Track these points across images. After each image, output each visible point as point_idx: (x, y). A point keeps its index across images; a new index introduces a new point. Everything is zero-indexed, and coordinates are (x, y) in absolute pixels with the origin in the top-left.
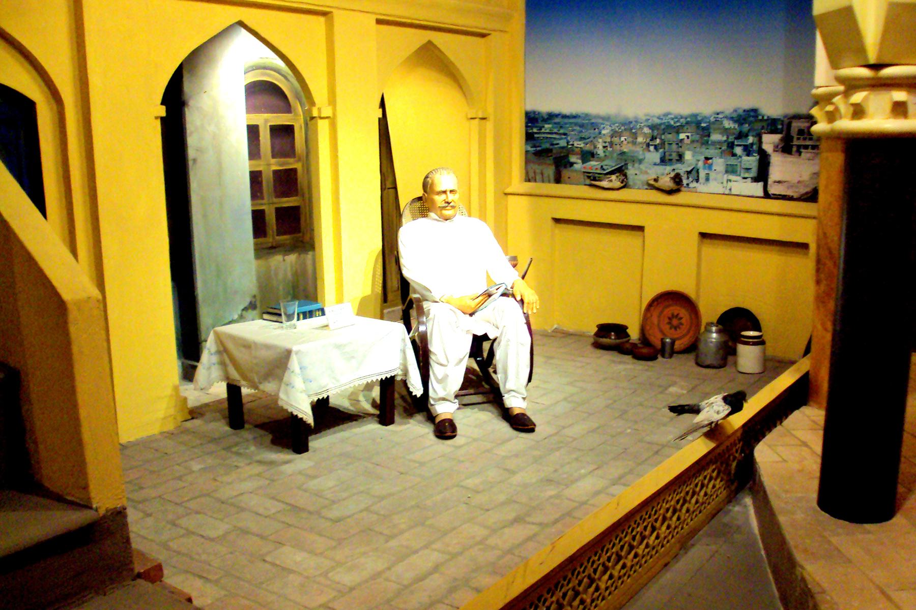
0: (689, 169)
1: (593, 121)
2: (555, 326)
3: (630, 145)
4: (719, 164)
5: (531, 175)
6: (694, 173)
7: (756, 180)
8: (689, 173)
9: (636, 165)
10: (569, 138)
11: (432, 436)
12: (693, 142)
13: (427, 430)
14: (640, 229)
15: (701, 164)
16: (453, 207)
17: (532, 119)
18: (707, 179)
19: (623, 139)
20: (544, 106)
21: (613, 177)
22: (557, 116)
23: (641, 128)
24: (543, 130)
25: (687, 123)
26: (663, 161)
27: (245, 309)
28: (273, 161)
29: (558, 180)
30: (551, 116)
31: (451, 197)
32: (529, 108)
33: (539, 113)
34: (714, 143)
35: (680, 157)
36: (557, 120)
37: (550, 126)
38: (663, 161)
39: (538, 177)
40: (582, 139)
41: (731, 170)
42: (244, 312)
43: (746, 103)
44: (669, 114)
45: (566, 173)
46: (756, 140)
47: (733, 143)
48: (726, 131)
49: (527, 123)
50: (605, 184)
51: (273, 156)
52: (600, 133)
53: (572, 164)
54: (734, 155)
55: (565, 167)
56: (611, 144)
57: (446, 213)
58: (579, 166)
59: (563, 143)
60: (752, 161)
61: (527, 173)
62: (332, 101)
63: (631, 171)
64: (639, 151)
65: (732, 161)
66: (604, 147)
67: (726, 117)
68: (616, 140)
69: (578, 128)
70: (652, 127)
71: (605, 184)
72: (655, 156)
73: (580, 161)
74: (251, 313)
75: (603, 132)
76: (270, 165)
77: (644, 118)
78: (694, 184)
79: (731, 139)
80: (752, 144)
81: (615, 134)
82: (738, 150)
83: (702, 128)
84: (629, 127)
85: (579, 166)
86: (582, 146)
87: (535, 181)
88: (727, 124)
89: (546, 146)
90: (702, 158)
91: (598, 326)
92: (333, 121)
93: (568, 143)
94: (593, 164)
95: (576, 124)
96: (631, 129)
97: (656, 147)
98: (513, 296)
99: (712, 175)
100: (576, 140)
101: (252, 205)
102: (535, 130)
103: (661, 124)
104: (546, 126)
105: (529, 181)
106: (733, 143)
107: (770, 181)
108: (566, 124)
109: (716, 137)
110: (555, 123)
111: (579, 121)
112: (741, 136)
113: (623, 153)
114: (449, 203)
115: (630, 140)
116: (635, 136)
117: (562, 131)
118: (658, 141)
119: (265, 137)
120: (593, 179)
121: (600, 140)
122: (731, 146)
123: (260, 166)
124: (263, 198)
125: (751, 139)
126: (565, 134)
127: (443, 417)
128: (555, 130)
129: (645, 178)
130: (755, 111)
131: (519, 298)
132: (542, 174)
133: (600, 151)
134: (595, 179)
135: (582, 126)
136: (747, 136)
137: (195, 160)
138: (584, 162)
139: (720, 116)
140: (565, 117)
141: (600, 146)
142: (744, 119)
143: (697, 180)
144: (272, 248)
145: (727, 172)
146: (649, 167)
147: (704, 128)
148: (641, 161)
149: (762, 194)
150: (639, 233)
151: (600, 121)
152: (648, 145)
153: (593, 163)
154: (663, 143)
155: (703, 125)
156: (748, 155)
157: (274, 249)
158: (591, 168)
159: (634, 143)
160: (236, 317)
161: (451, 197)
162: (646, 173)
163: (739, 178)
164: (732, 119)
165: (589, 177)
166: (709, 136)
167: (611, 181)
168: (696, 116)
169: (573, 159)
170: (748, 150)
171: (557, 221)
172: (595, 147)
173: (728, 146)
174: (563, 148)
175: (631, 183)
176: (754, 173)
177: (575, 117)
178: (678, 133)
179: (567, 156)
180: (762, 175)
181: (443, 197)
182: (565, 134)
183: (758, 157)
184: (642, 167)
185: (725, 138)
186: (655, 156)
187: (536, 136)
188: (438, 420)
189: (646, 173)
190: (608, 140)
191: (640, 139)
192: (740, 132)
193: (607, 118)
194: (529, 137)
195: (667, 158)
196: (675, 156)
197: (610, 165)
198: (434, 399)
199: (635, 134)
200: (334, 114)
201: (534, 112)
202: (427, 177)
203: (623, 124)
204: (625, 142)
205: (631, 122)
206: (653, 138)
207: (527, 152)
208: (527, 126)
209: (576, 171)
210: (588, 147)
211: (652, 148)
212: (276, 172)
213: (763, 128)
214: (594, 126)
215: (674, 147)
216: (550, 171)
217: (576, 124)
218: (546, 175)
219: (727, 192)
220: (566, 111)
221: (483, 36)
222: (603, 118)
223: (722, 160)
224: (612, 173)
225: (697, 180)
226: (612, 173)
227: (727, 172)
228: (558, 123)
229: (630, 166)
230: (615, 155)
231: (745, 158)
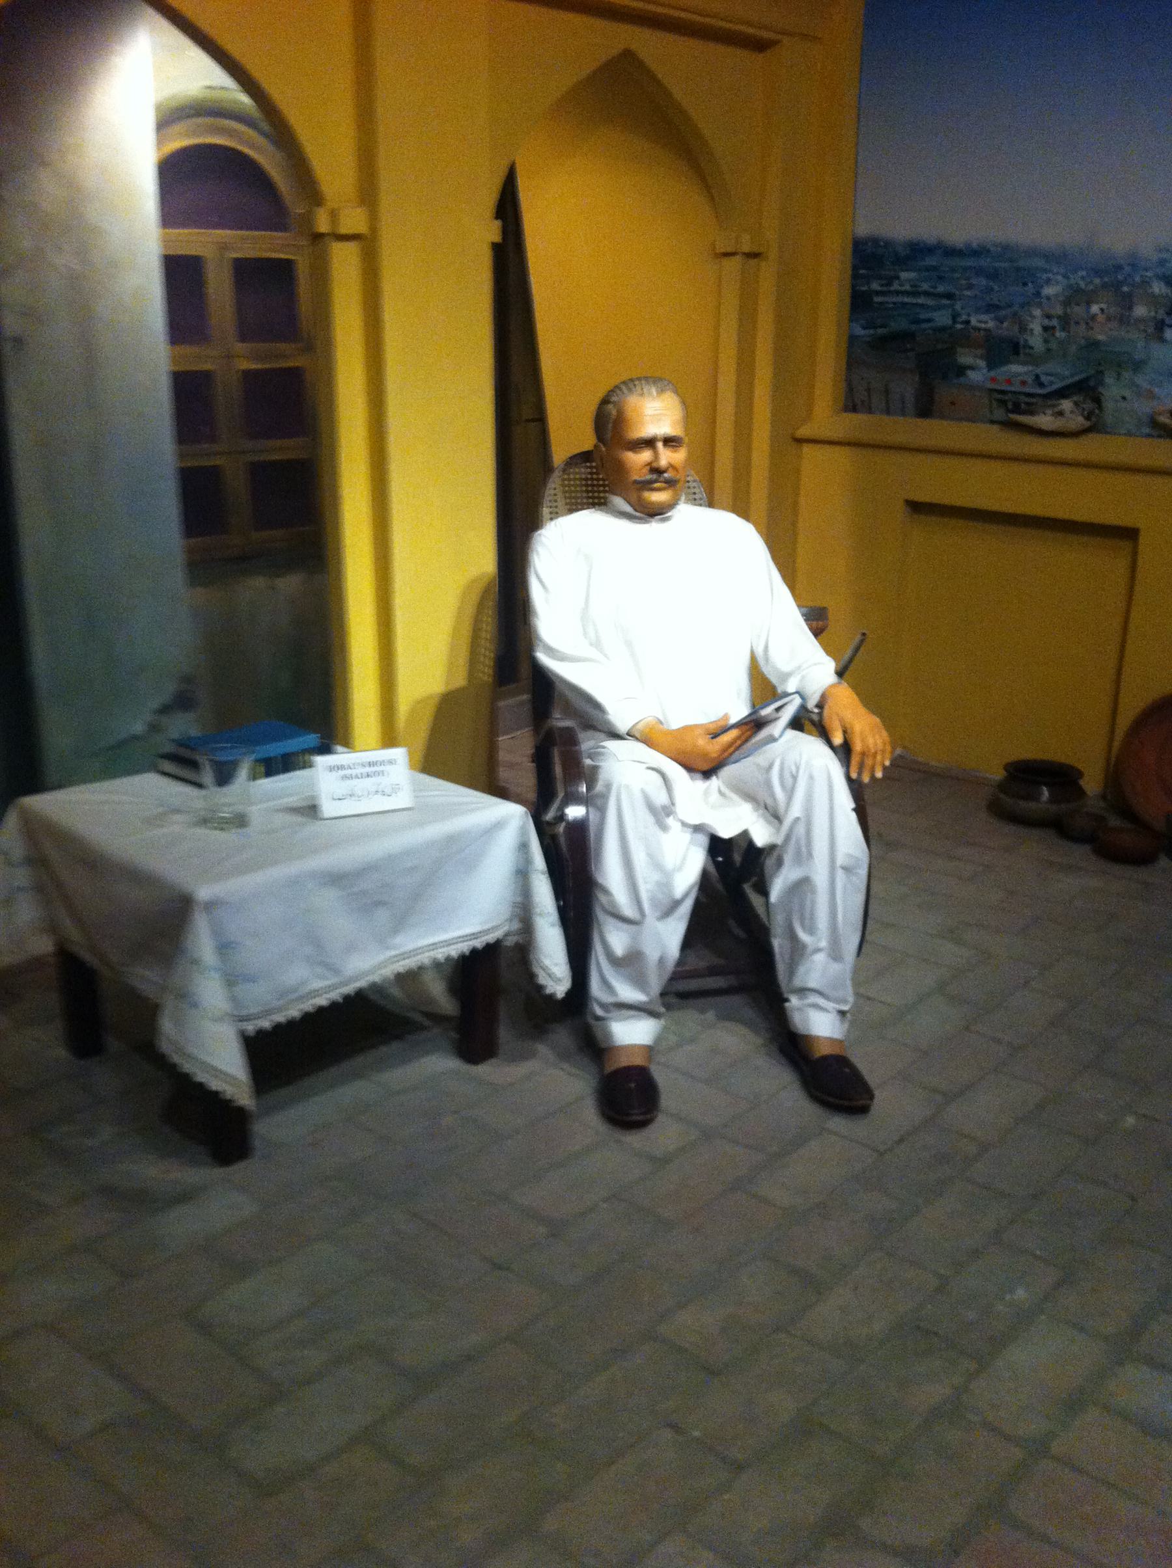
1: (1021, 263)
3: (1114, 324)
9: (1126, 375)
10: (958, 307)
11: (590, 1113)
14: (1130, 534)
16: (671, 483)
17: (870, 258)
19: (1095, 309)
20: (902, 223)
21: (1066, 405)
23: (1146, 283)
24: (896, 286)
27: (165, 710)
28: (240, 347)
29: (925, 409)
30: (917, 251)
31: (666, 457)
32: (863, 229)
33: (888, 244)
36: (930, 261)
37: (912, 275)
40: (991, 308)
49: (855, 268)
50: (1044, 420)
51: (243, 338)
52: (1038, 294)
53: (961, 370)
57: (658, 497)
58: (979, 374)
59: (942, 318)
61: (850, 390)
62: (368, 194)
63: (1112, 390)
66: (1046, 329)
68: (1078, 310)
69: (983, 282)
71: (1044, 420)
73: (982, 363)
76: (233, 358)
77: (1155, 257)
81: (1076, 296)
84: (1116, 280)
85: (979, 374)
86: (991, 325)
87: (870, 411)
89: (900, 324)
91: (1007, 767)
92: (368, 245)
93: (955, 317)
95: (979, 272)
96: (1117, 286)
98: (824, 733)
100: (978, 310)
101: (182, 456)
102: (875, 286)
104: (904, 275)
108: (953, 270)
110: (927, 269)
111: (984, 262)
113: (1094, 345)
114: (658, 471)
116: (1127, 302)
117: (941, 289)
119: (219, 288)
120: (1012, 409)
121: (1037, 312)
123: (202, 359)
124: (213, 439)
126: (949, 296)
127: (624, 1061)
128: (925, 286)
129: (1144, 407)
131: (838, 740)
132: (887, 392)
133: (1036, 340)
134: (1017, 409)
135: (994, 275)
138: (990, 367)
140: (951, 252)
148: (1138, 366)
150: (1126, 545)
151: (1039, 263)
153: (1015, 368)
157: (245, 562)
158: (1009, 382)
160: (138, 728)
161: (666, 457)
162: (1151, 396)
165: (1002, 403)
167: (1061, 414)
169: (965, 357)
171: (916, 507)
172: (1023, 329)
174: (943, 329)
175: (1109, 419)
181: (646, 456)
184: (1141, 380)
188: (610, 1067)
189: (1151, 396)
190: (1059, 311)
191: (1140, 311)
193: (1058, 258)
194: (860, 303)
197: (1060, 373)
198: (604, 1006)
199: (1129, 295)
200: (374, 229)
201: (875, 241)
202: (605, 401)
203: (1097, 272)
204: (1101, 318)
205: (1119, 268)
207: (852, 339)
208: (855, 276)
209: (972, 387)
210: (1008, 329)
212: (247, 374)
214: (1025, 276)
216: (906, 387)
217: (979, 272)
221: (760, 46)
222: (1048, 256)
224: (1062, 393)
228: (935, 268)
229: (1109, 380)
230: (1073, 348)
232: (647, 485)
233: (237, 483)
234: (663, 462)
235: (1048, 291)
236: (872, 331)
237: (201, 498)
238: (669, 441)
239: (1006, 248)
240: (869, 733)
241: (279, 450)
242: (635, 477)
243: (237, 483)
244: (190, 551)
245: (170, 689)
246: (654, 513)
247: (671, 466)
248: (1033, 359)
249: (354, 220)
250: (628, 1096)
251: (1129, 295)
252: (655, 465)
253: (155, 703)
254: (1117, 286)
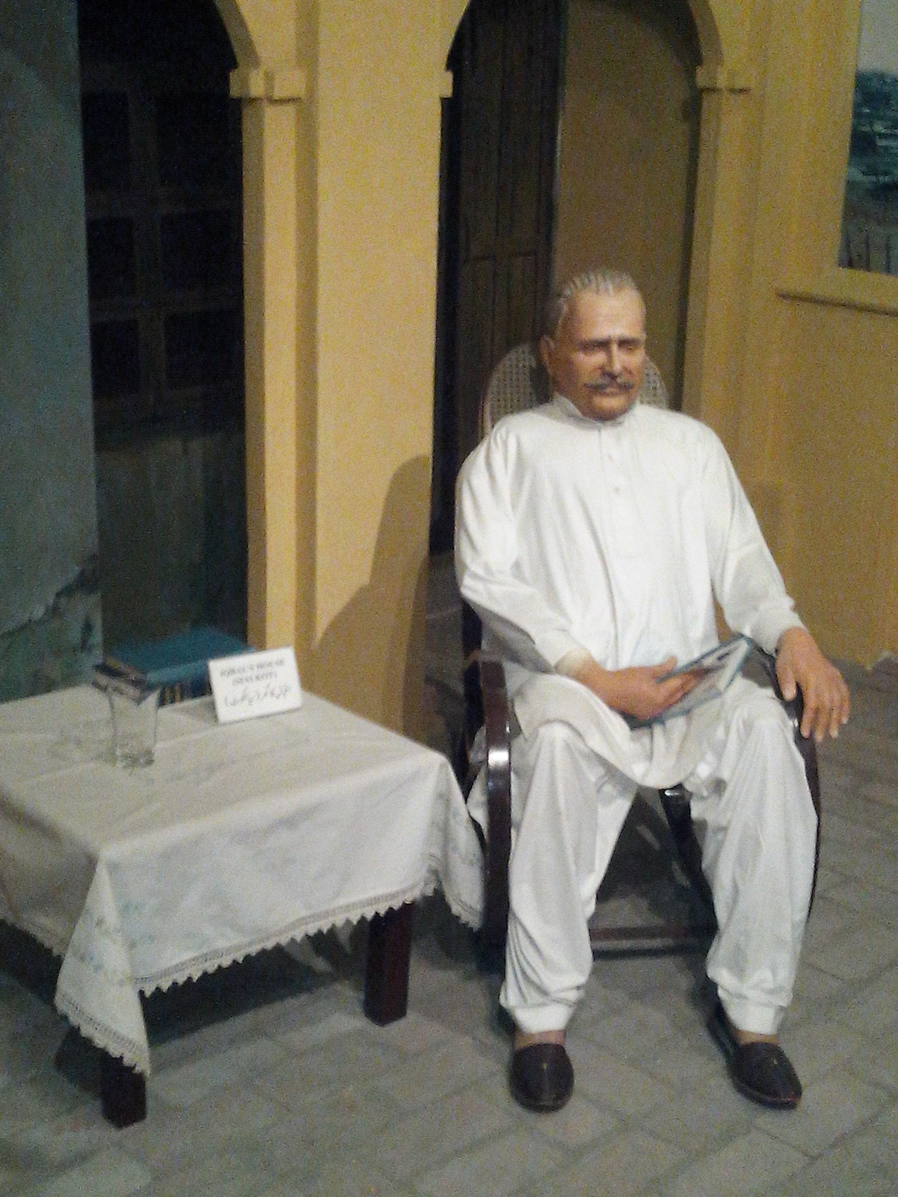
2: (886, 654)
11: (499, 1088)
13: (486, 1067)
16: (626, 388)
31: (620, 360)
32: (870, 62)
39: (877, 257)
42: (63, 600)
49: (857, 106)
61: (847, 242)
62: (308, 55)
87: (868, 267)
92: (305, 108)
101: (94, 311)
102: (879, 128)
105: (850, 264)
114: (613, 377)
131: (790, 693)
132: (888, 248)
160: (39, 612)
161: (620, 360)
181: (599, 358)
187: (881, 143)
188: (521, 1044)
194: (862, 144)
200: (312, 90)
201: (881, 77)
207: (851, 185)
208: (857, 115)
232: (598, 389)
234: (617, 367)
236: (874, 178)
237: (114, 361)
238: (625, 344)
240: (826, 689)
242: (585, 379)
246: (607, 417)
247: (626, 370)
249: (290, 83)
250: (539, 1076)
252: (607, 369)
253: (57, 587)
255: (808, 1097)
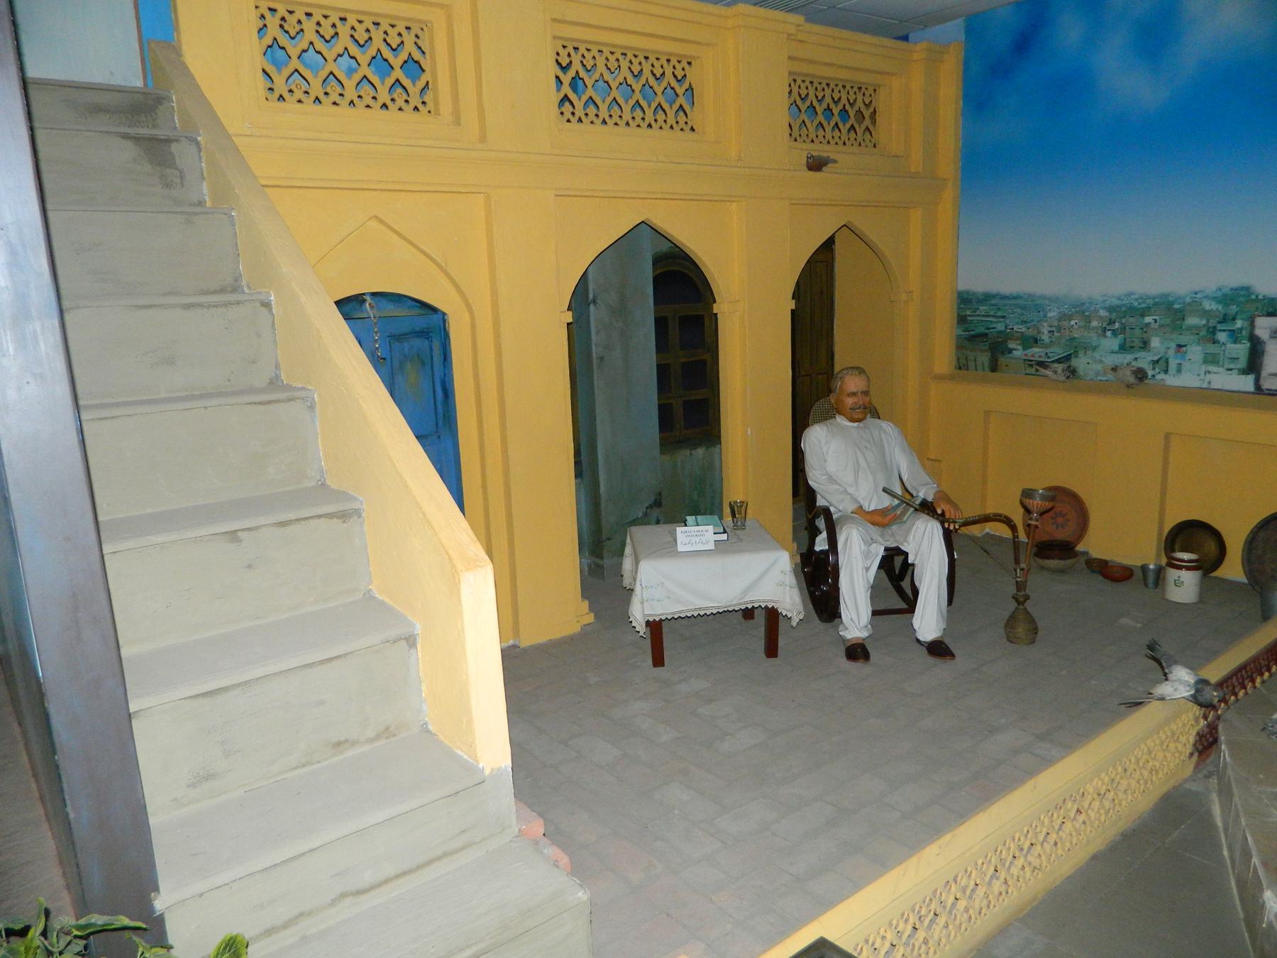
0: (1156, 358)
1: (1038, 302)
4: (1195, 352)
5: (963, 361)
6: (1162, 363)
7: (1245, 372)
8: (1155, 362)
9: (1089, 352)
12: (1161, 326)
15: (1171, 352)
18: (1179, 370)
19: (1073, 323)
22: (994, 296)
23: (1096, 311)
25: (1156, 304)
26: (1123, 348)
27: (650, 507)
29: (994, 368)
30: (987, 297)
32: (962, 287)
33: (974, 294)
34: (1190, 328)
35: (1145, 345)
38: (1123, 348)
39: (971, 364)
40: (1024, 322)
41: (1210, 359)
43: (1232, 278)
44: (1132, 294)
45: (1002, 360)
46: (1246, 324)
47: (1215, 327)
48: (1206, 314)
53: (1010, 351)
54: (1215, 342)
55: (1003, 353)
56: (1059, 329)
59: (1000, 327)
60: (1241, 350)
64: (1094, 338)
65: (1211, 349)
67: (1207, 297)
70: (1111, 309)
72: (1112, 343)
74: (655, 513)
75: (1050, 315)
78: (1162, 376)
79: (1213, 323)
80: (1241, 330)
81: (1064, 317)
82: (1222, 337)
83: (1173, 313)
84: (1082, 311)
85: (1019, 353)
88: (1208, 305)
89: (981, 330)
90: (1173, 345)
94: (1036, 352)
96: (1084, 312)
97: (1115, 333)
99: (1186, 365)
102: (968, 312)
103: (1120, 307)
106: (1215, 327)
107: (1264, 374)
109: (1192, 321)
111: (1021, 302)
112: (1225, 319)
115: (1082, 323)
116: (1088, 320)
118: (1117, 325)
122: (1213, 331)
125: (1239, 324)
126: (1003, 317)
130: (1247, 289)
135: (1024, 308)
136: (1234, 319)
137: (602, 358)
138: (1024, 349)
139: (1199, 296)
140: (1004, 297)
141: (1045, 330)
142: (1232, 299)
143: (1166, 372)
144: (679, 442)
145: (1205, 362)
146: (1105, 354)
147: (1176, 311)
148: (1094, 349)
149: (1251, 388)
152: (1104, 330)
153: (1036, 350)
154: (1123, 329)
155: (1177, 306)
156: (1235, 342)
159: (1087, 327)
160: (640, 515)
162: (1101, 361)
163: (1221, 369)
164: (1214, 298)
166: (1183, 319)
168: (1167, 296)
169: (1011, 345)
170: (1235, 336)
172: (1039, 332)
173: (1208, 331)
176: (1243, 363)
177: (1015, 298)
178: (1143, 316)
179: (1005, 342)
180: (1254, 365)
182: (1003, 317)
183: (1248, 345)
184: (1097, 355)
185: (1204, 322)
186: (1112, 343)
189: (1101, 361)
191: (1094, 324)
192: (1225, 315)
193: (1054, 299)
194: (962, 320)
195: (1128, 345)
196: (1137, 343)
197: (1058, 351)
201: (968, 292)
206: (1111, 322)
207: (959, 337)
208: (959, 308)
210: (1031, 332)
211: (1109, 334)
212: (683, 364)
213: (1257, 309)
214: (1039, 308)
215: (1138, 332)
216: (985, 358)
218: (979, 362)
219: (1205, 385)
220: (1006, 289)
222: (1050, 299)
223: (1199, 348)
224: (1059, 361)
225: (1166, 372)
226: (1059, 361)
227: (1205, 362)
229: (1081, 354)
231: (1230, 346)
233: (678, 410)
235: (1050, 315)
239: (1030, 295)
241: (696, 395)
243: (678, 410)
244: (661, 439)
245: (653, 498)
248: (1046, 346)
251: (1088, 317)
254: (1084, 312)
255: (957, 659)
